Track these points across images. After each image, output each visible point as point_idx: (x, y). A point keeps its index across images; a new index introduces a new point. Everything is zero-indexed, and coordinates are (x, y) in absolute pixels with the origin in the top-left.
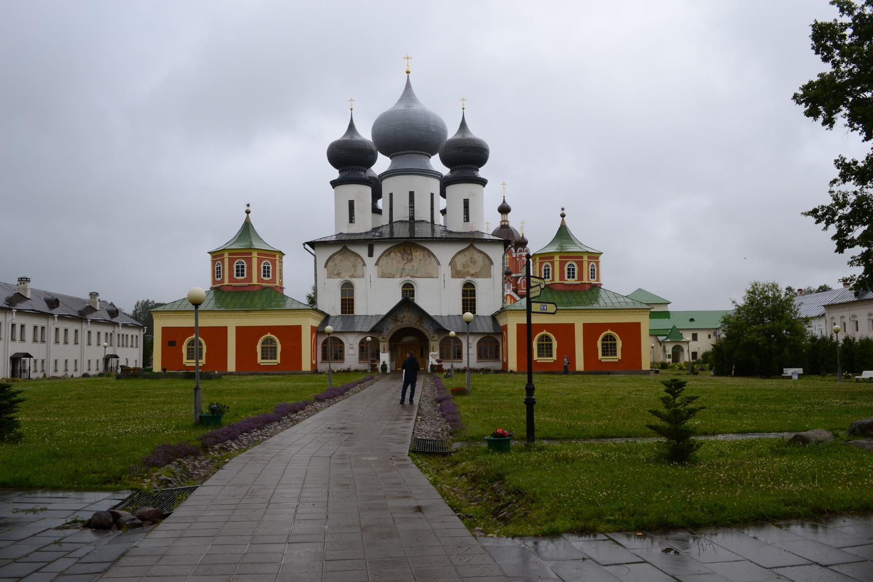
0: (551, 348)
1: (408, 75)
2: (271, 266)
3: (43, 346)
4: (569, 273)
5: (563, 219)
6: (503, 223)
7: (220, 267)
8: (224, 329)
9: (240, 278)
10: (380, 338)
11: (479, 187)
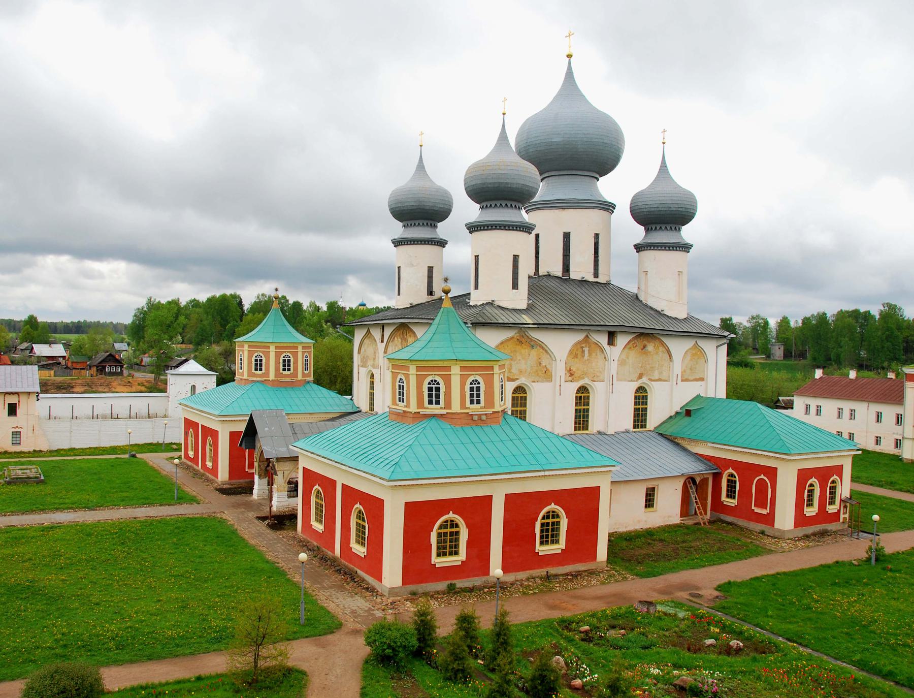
1: (570, 60)
2: (292, 359)
4: (430, 396)
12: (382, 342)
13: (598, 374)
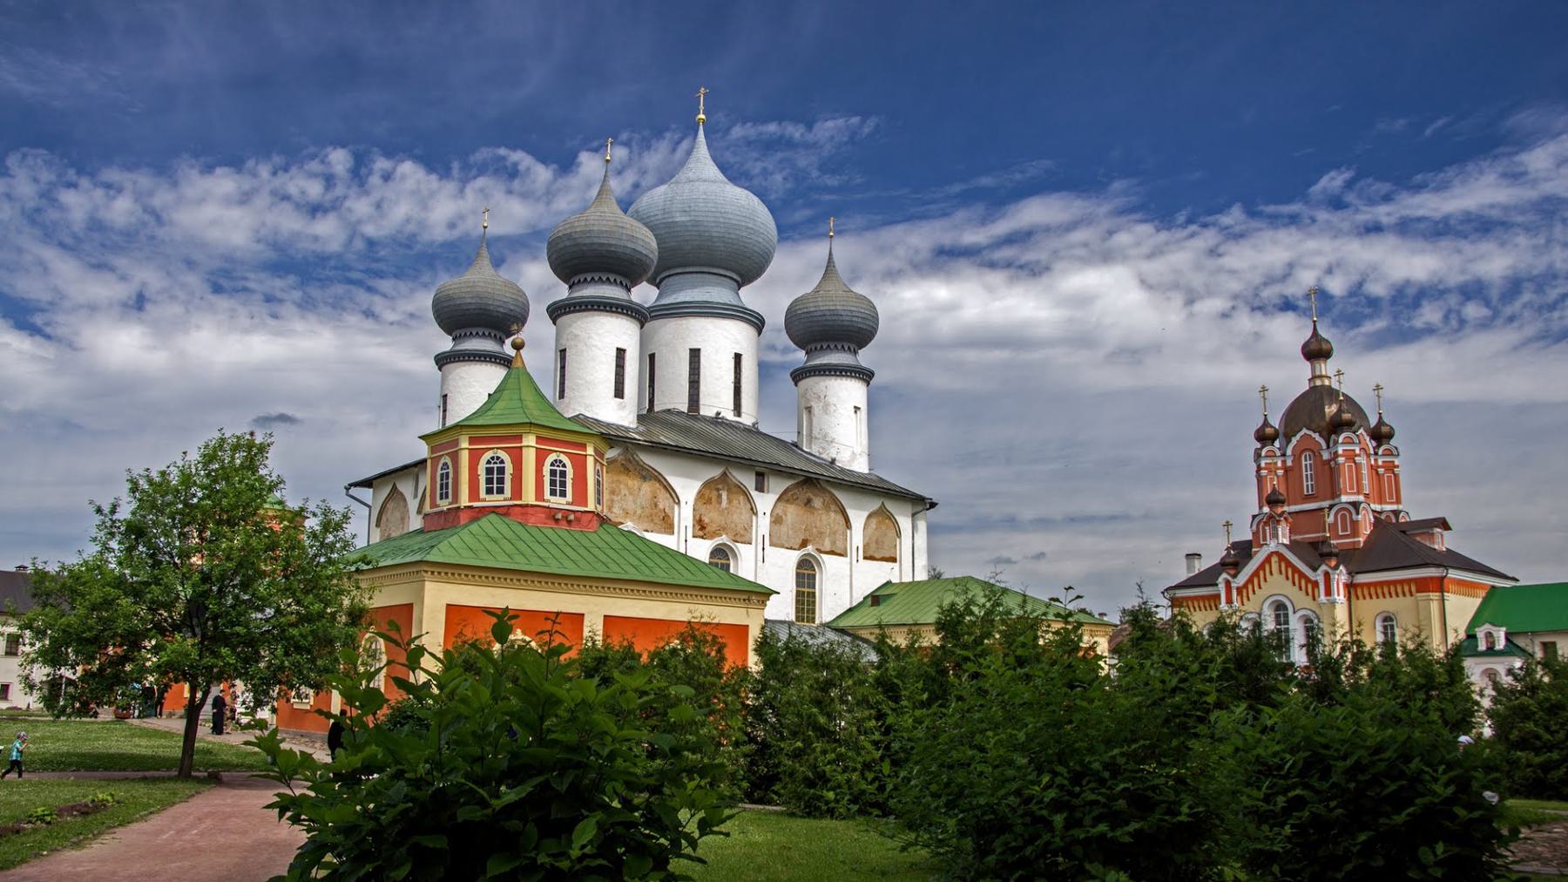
4: (489, 481)
12: (416, 496)
13: (742, 532)
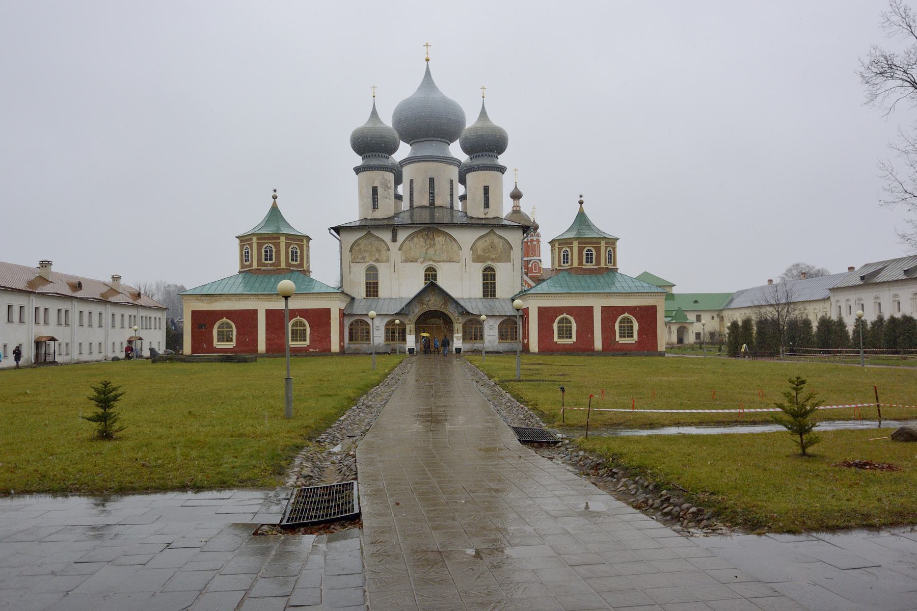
0: (571, 330)
2: (298, 251)
3: (68, 329)
4: (587, 258)
5: (581, 206)
6: (515, 209)
7: (248, 252)
8: (255, 312)
9: (269, 262)
10: (406, 322)
11: (499, 174)
